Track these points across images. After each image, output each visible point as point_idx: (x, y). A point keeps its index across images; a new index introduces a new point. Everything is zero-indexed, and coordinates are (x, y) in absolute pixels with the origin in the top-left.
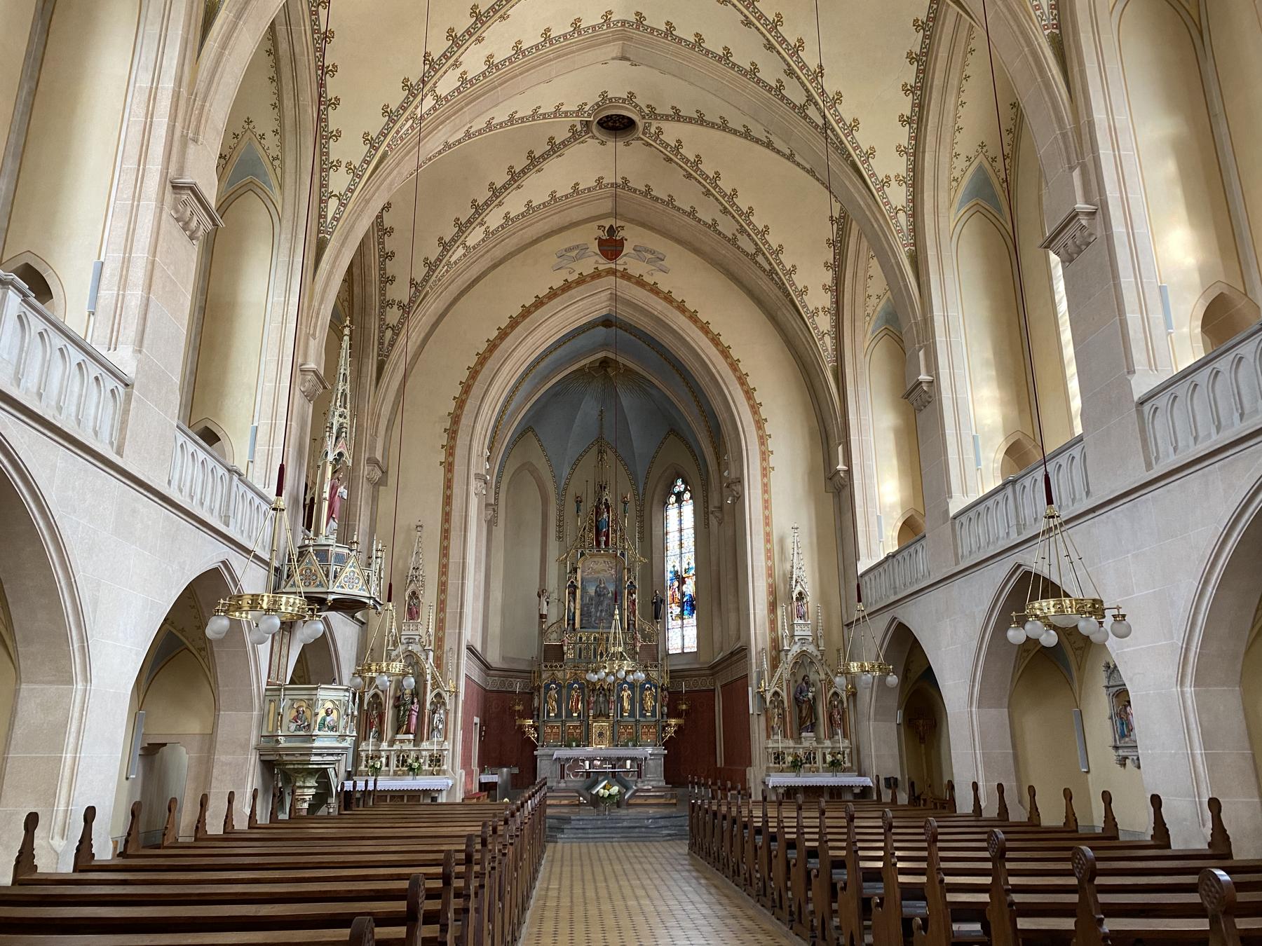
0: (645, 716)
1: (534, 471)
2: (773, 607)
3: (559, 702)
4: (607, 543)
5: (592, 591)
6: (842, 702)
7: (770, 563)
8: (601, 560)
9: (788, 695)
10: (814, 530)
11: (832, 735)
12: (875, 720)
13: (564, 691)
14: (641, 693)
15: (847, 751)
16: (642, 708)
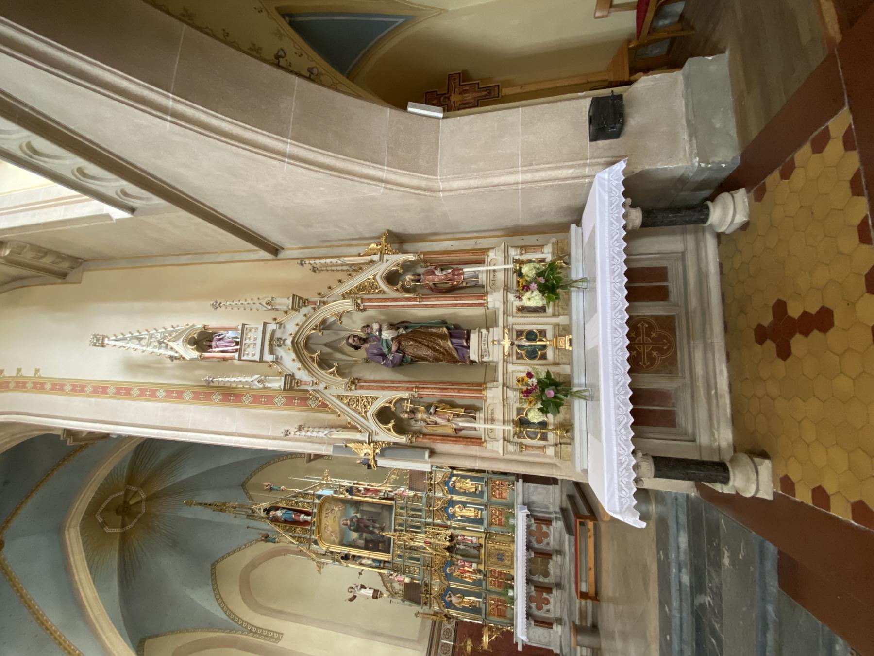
0: (482, 492)
1: (253, 565)
2: (230, 395)
3: (465, 593)
4: (308, 514)
5: (354, 535)
6: (407, 267)
7: (161, 393)
8: (324, 521)
9: (383, 385)
10: (126, 305)
11: (477, 289)
12: (432, 171)
13: (454, 585)
14: (458, 493)
15: (514, 253)
16: (474, 494)
